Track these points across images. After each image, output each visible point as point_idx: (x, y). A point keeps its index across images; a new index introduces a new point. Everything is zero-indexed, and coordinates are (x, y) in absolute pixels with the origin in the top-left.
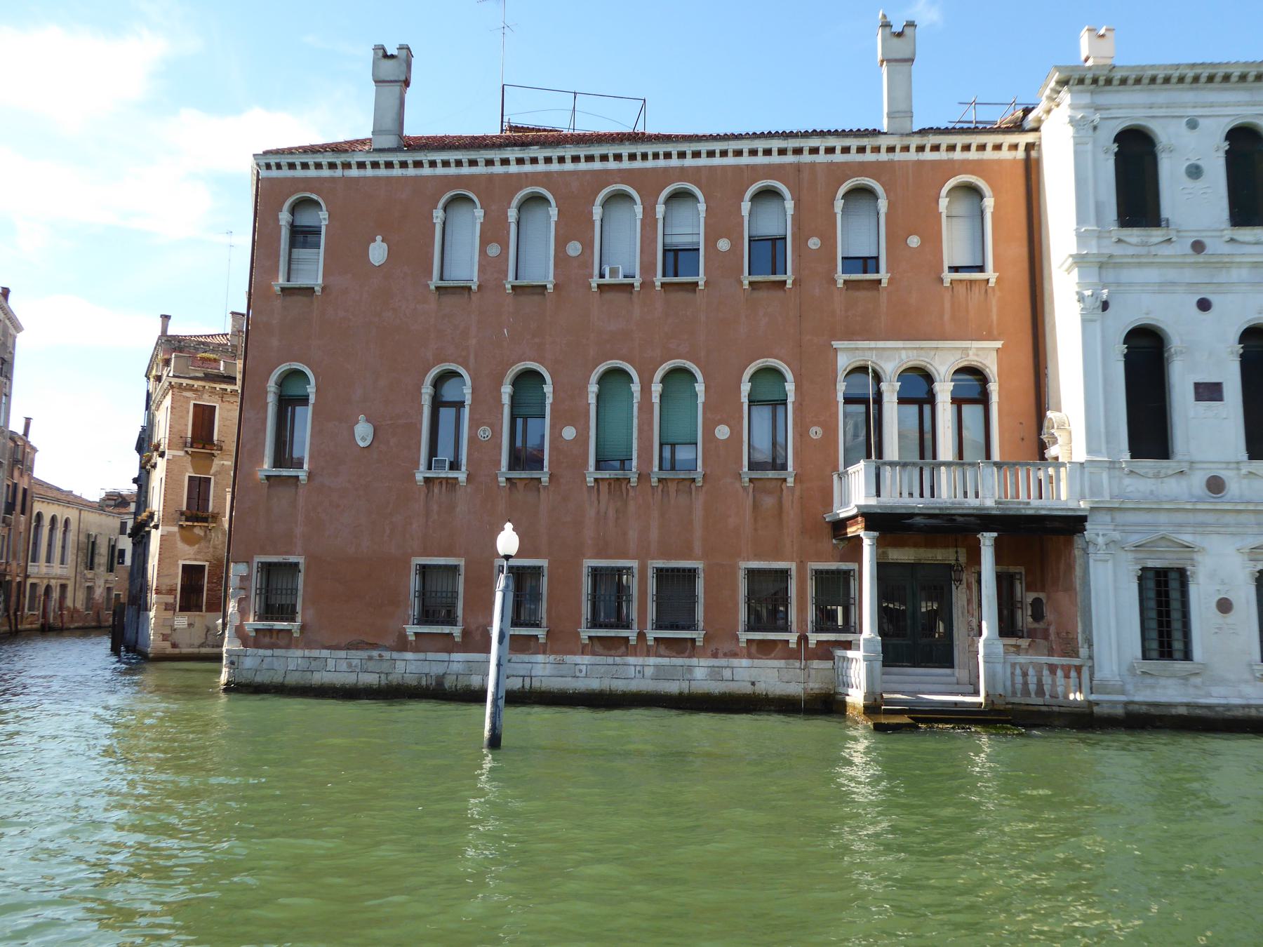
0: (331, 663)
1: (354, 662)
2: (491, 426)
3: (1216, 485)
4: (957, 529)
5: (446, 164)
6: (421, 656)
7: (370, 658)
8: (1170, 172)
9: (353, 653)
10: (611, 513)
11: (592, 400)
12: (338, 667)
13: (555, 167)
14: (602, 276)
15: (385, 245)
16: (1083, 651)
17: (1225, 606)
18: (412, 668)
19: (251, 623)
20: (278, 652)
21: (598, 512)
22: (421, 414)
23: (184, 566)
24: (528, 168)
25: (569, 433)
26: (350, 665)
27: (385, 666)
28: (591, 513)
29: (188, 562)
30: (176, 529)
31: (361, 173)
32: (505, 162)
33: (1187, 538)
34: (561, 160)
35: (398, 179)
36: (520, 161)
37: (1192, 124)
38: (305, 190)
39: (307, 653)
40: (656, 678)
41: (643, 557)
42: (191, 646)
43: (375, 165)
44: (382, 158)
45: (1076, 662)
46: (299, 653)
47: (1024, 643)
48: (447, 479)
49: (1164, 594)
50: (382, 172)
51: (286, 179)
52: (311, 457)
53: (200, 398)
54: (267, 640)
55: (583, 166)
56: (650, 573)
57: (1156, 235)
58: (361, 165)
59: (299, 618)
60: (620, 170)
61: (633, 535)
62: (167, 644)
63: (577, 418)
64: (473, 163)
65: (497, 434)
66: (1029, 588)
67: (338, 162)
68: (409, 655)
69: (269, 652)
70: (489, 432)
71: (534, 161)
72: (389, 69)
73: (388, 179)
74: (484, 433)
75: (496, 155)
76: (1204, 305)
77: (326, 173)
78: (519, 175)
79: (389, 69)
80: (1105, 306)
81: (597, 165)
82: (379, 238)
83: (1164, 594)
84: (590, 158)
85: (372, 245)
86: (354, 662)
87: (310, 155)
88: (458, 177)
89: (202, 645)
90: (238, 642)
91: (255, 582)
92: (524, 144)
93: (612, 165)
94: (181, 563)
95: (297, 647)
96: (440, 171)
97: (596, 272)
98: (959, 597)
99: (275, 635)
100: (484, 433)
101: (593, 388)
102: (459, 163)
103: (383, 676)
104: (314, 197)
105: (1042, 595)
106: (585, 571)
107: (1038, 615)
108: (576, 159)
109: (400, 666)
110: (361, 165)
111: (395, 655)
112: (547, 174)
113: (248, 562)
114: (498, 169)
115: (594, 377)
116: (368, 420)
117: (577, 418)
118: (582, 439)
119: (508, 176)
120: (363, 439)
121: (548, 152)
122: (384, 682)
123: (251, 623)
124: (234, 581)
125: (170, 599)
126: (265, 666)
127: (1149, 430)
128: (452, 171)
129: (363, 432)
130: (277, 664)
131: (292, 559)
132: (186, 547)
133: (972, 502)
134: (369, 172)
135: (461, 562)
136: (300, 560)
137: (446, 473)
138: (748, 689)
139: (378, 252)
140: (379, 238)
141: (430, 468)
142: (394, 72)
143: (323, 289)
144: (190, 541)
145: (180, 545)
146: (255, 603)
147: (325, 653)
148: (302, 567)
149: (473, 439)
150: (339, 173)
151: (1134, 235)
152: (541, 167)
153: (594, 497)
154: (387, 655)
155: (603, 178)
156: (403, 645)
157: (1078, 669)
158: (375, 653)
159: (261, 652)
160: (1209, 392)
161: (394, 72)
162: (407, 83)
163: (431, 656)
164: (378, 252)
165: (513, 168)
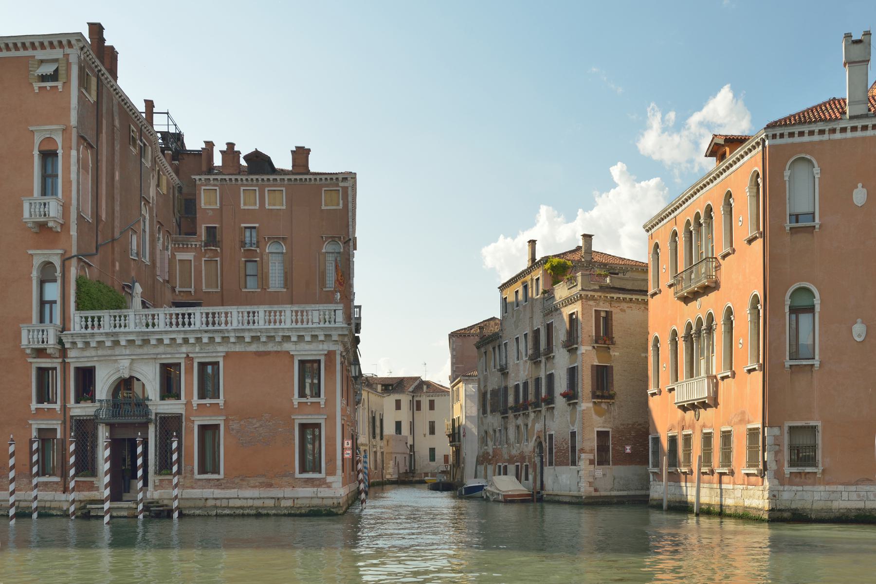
9: (860, 488)
30: (591, 405)
42: (606, 490)
54: (798, 480)
59: (820, 465)
89: (611, 490)
94: (596, 429)
99: (803, 476)
131: (812, 423)
132: (599, 418)
144: (599, 414)
145: (595, 417)
148: (820, 429)
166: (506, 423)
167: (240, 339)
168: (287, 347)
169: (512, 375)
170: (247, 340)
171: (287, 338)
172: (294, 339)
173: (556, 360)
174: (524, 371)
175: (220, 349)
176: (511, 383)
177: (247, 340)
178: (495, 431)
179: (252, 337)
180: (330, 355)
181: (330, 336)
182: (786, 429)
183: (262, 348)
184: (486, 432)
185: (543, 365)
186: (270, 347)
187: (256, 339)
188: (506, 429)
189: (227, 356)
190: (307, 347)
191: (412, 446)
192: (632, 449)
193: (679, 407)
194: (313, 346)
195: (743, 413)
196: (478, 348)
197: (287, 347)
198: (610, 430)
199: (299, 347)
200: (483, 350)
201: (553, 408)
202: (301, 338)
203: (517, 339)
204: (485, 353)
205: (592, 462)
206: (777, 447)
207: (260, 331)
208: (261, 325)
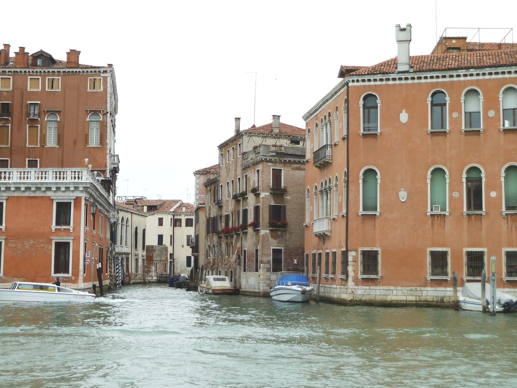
0: (395, 292)
1: (405, 291)
2: (459, 192)
5: (432, 77)
6: (434, 289)
7: (411, 290)
10: (514, 228)
11: (503, 179)
12: (397, 294)
13: (481, 77)
14: (504, 125)
15: (407, 114)
18: (430, 294)
19: (360, 276)
20: (372, 287)
21: (508, 228)
22: (427, 187)
23: (273, 250)
24: (469, 78)
25: (493, 194)
26: (403, 293)
27: (419, 293)
28: (505, 228)
29: (275, 248)
31: (394, 82)
32: (458, 76)
34: (484, 74)
35: (410, 84)
36: (465, 75)
38: (369, 91)
39: (384, 288)
43: (400, 79)
44: (403, 76)
46: (381, 288)
48: (440, 215)
50: (403, 82)
51: (361, 86)
52: (380, 206)
53: (275, 166)
55: (494, 77)
58: (394, 79)
60: (510, 78)
62: (269, 288)
63: (497, 188)
64: (444, 77)
65: (461, 195)
67: (384, 78)
68: (429, 289)
69: (368, 287)
70: (458, 195)
71: (472, 75)
72: (403, 36)
73: (406, 84)
74: (456, 195)
75: (454, 73)
77: (378, 83)
78: (465, 81)
79: (403, 36)
81: (500, 76)
82: (404, 111)
84: (497, 73)
85: (401, 114)
86: (405, 291)
87: (372, 76)
88: (437, 82)
90: (354, 283)
91: (360, 258)
92: (467, 68)
93: (507, 76)
95: (380, 285)
96: (429, 80)
97: (502, 123)
100: (456, 195)
101: (503, 174)
102: (438, 77)
103: (417, 297)
104: (374, 93)
106: (503, 253)
108: (490, 74)
109: (425, 293)
110: (394, 79)
111: (422, 288)
112: (478, 81)
113: (356, 251)
114: (455, 79)
115: (503, 171)
116: (405, 190)
117: (497, 188)
118: (499, 197)
119: (460, 82)
120: (403, 198)
121: (478, 71)
122: (418, 300)
123: (360, 276)
124: (350, 259)
125: (268, 266)
126: (366, 293)
128: (435, 80)
129: (403, 195)
130: (373, 293)
131: (375, 249)
134: (398, 82)
135: (448, 249)
136: (379, 249)
137: (439, 212)
139: (404, 117)
140: (404, 111)
141: (432, 210)
142: (404, 33)
143: (380, 133)
146: (360, 268)
147: (392, 288)
148: (380, 252)
149: (451, 198)
150: (384, 83)
152: (475, 78)
153: (506, 221)
154: (419, 288)
155: (504, 81)
156: (425, 285)
158: (413, 288)
159: (364, 287)
161: (404, 33)
162: (410, 41)
163: (438, 289)
164: (404, 117)
165: (462, 79)
166: (221, 241)
167: (18, 189)
168: (49, 194)
169: (224, 208)
170: (23, 189)
171: (49, 189)
172: (54, 189)
173: (248, 200)
174: (231, 206)
175: (4, 194)
176: (224, 213)
177: (23, 189)
178: (214, 246)
179: (26, 188)
180: (77, 200)
181: (78, 187)
182: (359, 252)
183: (32, 195)
184: (209, 246)
185: (241, 203)
186: (38, 194)
187: (28, 189)
188: (220, 245)
189: (8, 199)
190: (62, 194)
191: (172, 255)
192: (297, 262)
193: (316, 235)
194: (67, 194)
195: (341, 241)
196: (206, 186)
197: (49, 194)
198: (282, 248)
199: (57, 194)
200: (208, 188)
201: (247, 232)
202: (58, 189)
203: (228, 183)
204: (210, 190)
205: (268, 270)
206: (354, 263)
207: (32, 184)
208: (33, 180)
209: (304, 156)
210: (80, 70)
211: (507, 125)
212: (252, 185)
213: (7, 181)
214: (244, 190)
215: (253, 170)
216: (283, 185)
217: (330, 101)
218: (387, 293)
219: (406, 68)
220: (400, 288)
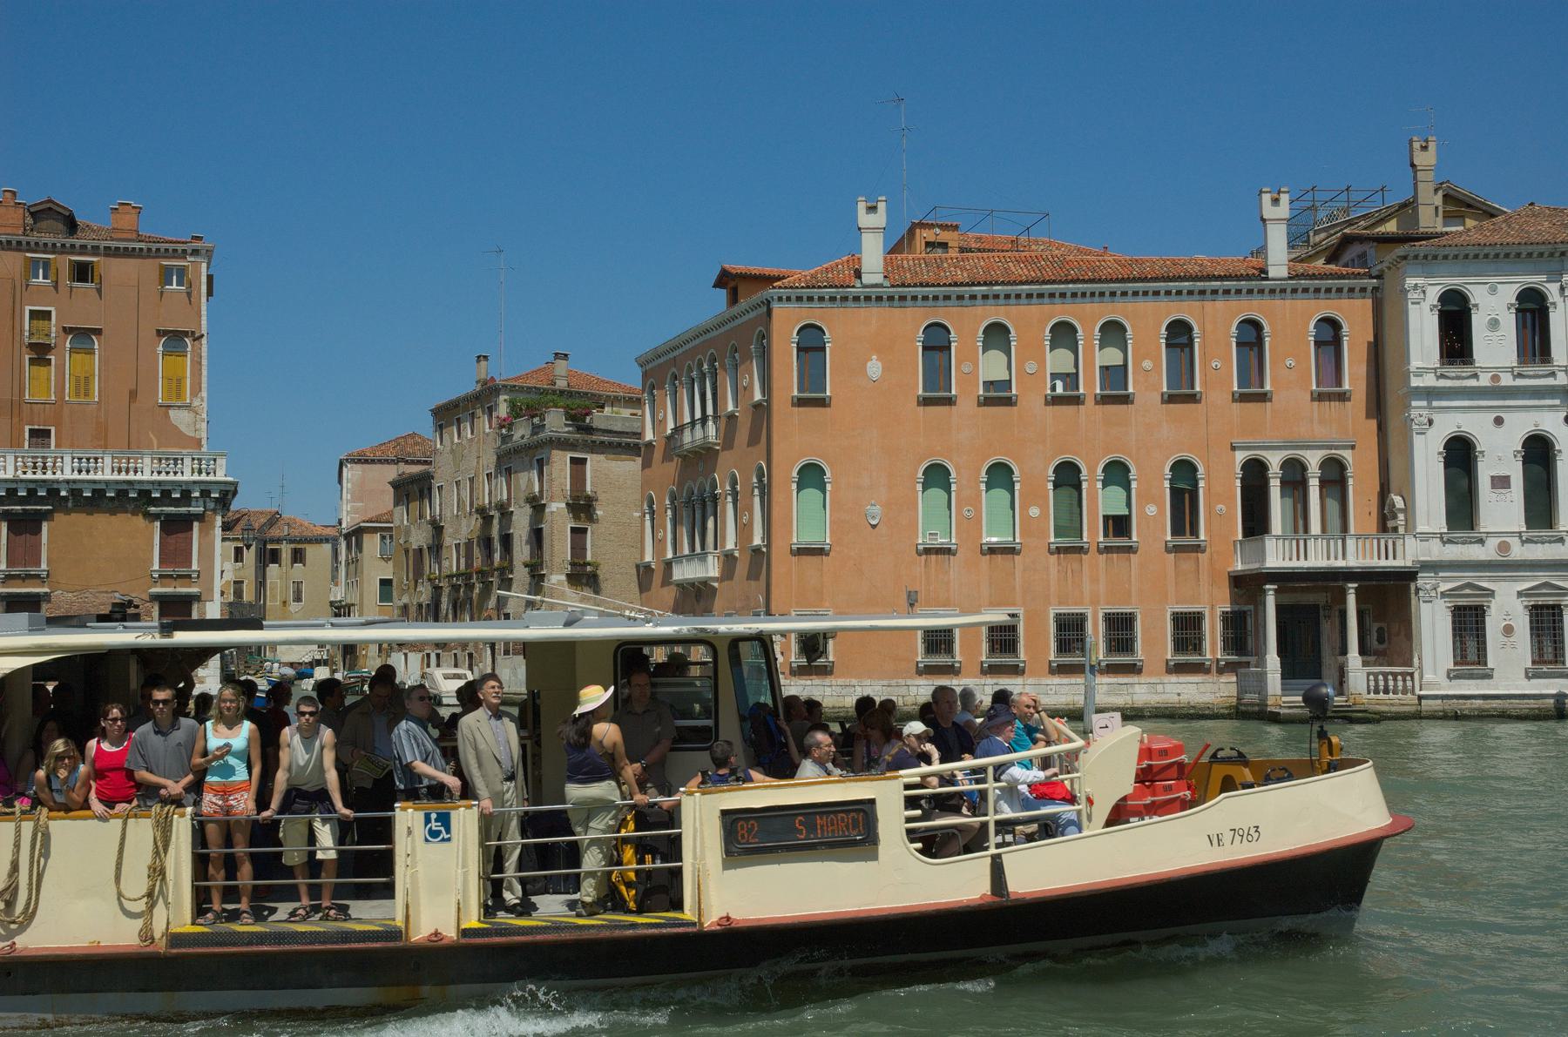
3: (1504, 547)
4: (1332, 580)
8: (1478, 321)
16: (1416, 660)
17: (1508, 630)
28: (1053, 571)
33: (1484, 585)
37: (1493, 290)
40: (1108, 693)
41: (1095, 602)
45: (1409, 670)
47: (1372, 658)
49: (1469, 623)
56: (1101, 615)
57: (1467, 371)
61: (1087, 587)
66: (1377, 619)
76: (1499, 421)
80: (1431, 422)
83: (1469, 623)
98: (1327, 628)
105: (1384, 625)
107: (1381, 640)
109: (913, 690)
127: (1462, 509)
133: (1340, 563)
138: (1175, 699)
139: (874, 368)
147: (854, 682)
151: (1452, 371)
157: (1412, 675)
160: (1501, 482)
164: (874, 368)
169: (448, 531)
173: (514, 518)
207: (107, 483)
209: (639, 435)
210: (142, 245)
211: (1060, 390)
212: (523, 487)
213: (49, 476)
214: (505, 497)
215: (527, 459)
216: (588, 488)
217: (715, 333)
218: (844, 692)
219: (879, 279)
220: (868, 682)
